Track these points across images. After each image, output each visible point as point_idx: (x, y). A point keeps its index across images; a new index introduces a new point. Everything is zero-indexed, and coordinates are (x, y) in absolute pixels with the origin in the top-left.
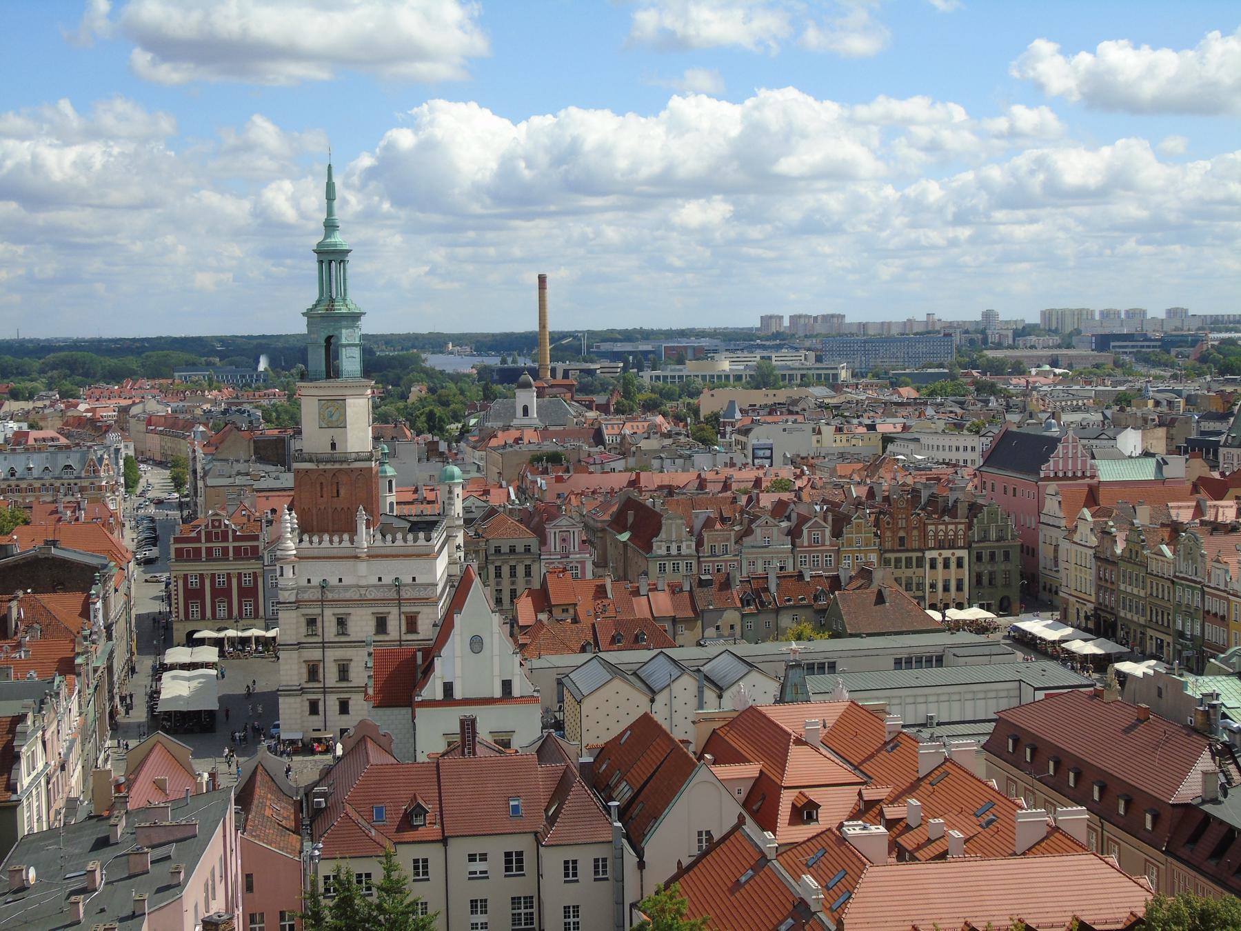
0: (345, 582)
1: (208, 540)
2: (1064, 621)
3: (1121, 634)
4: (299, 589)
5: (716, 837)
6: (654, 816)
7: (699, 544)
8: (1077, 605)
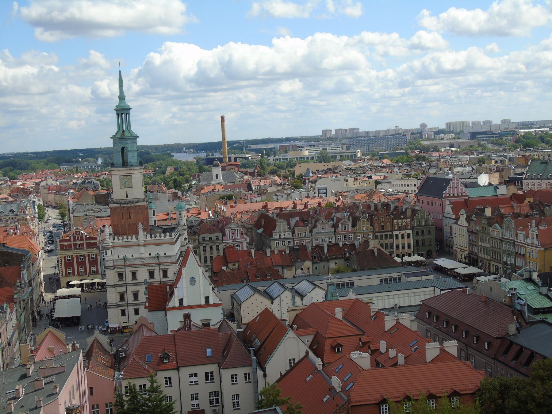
0: (134, 256)
1: (74, 240)
2: (455, 259)
3: (480, 264)
4: (114, 261)
5: (296, 361)
6: (270, 353)
7: (293, 233)
8: (461, 252)
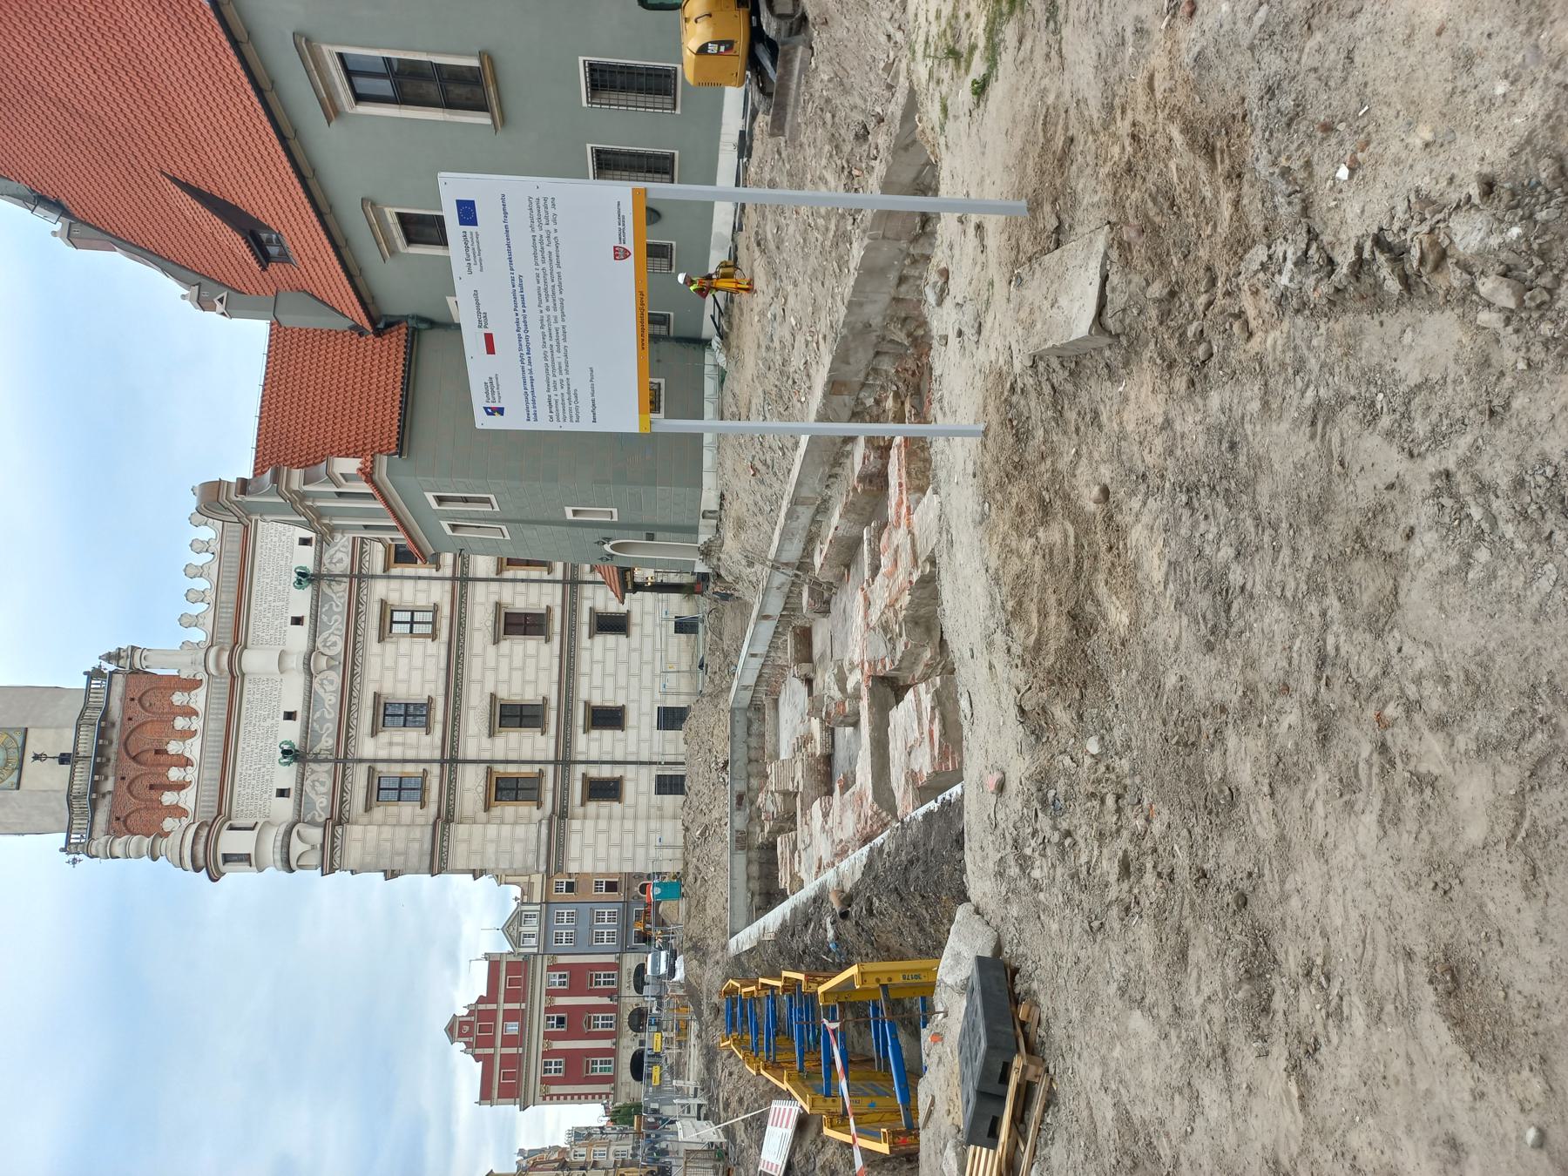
0: (296, 705)
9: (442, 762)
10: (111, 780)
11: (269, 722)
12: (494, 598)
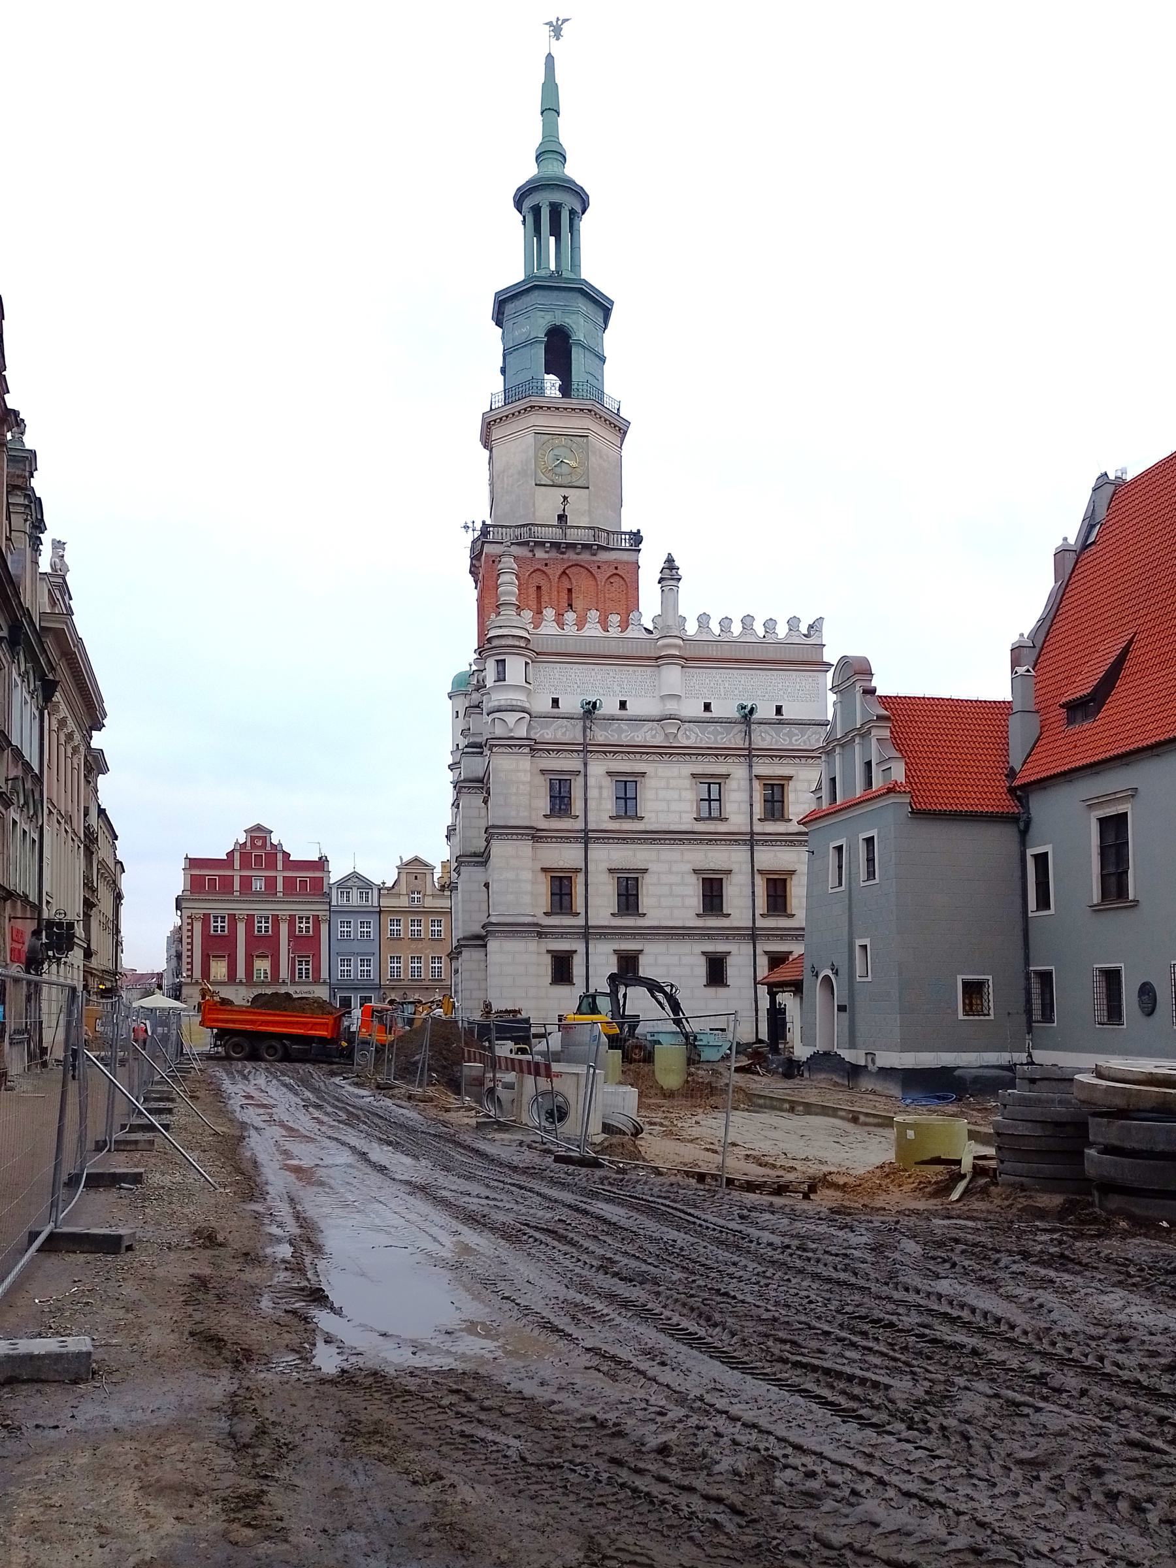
0: (633, 709)
9: (586, 831)
10: (546, 556)
11: (617, 689)
12: (735, 868)
